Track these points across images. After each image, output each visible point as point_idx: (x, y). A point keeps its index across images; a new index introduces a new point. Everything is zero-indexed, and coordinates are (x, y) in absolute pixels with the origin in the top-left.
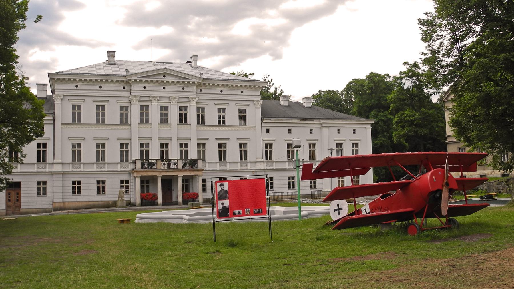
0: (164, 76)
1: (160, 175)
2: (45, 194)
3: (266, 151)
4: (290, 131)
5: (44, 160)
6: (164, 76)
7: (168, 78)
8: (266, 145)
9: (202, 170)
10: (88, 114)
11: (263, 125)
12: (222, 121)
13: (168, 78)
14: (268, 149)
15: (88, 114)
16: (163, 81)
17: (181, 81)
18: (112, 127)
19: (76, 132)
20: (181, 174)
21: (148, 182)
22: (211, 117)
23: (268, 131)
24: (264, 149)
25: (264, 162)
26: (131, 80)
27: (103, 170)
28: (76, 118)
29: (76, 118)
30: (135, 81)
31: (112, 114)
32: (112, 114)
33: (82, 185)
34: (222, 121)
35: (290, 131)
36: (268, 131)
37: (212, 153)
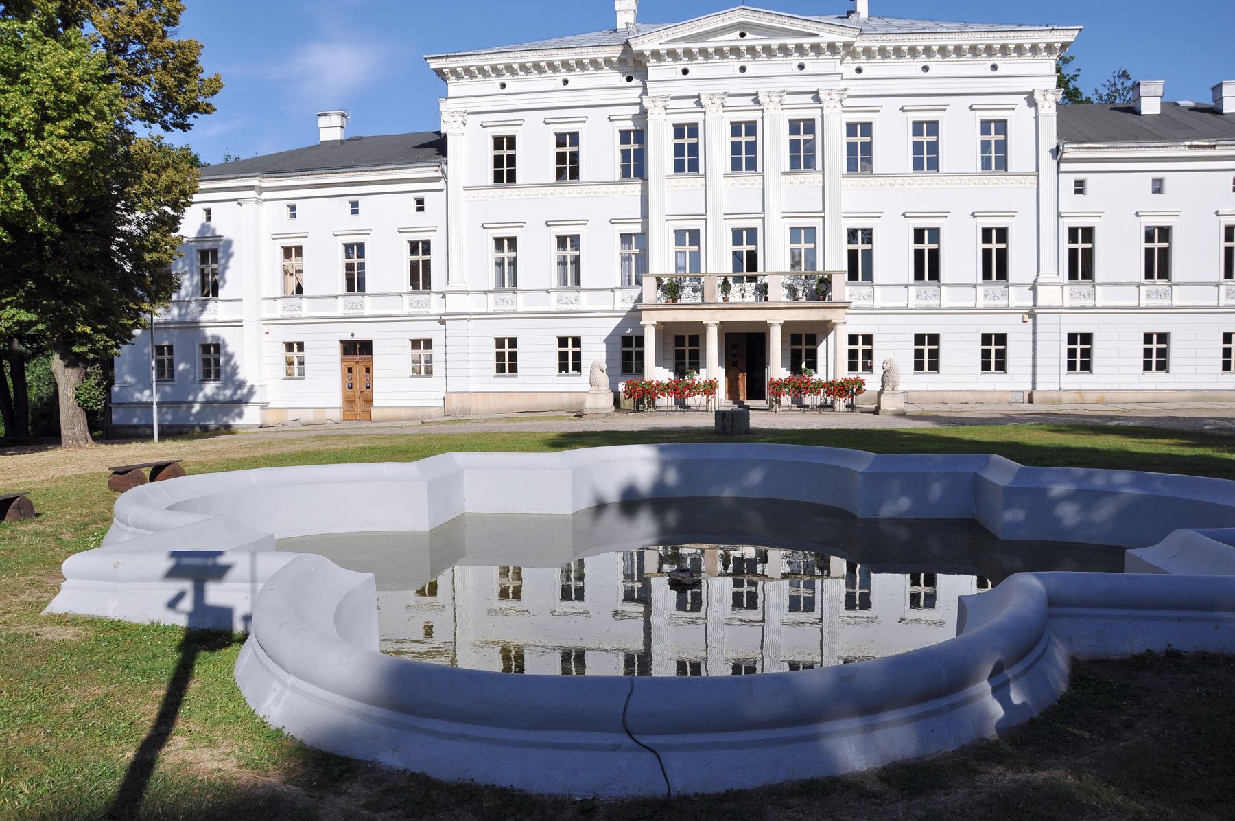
0: (742, 35)
1: (712, 320)
2: (429, 371)
3: (1073, 253)
4: (1158, 187)
5: (427, 284)
6: (742, 35)
7: (752, 39)
8: (1073, 233)
9: (844, 306)
10: (535, 158)
11: (1063, 167)
12: (926, 157)
13: (752, 39)
14: (1080, 246)
15: (535, 158)
16: (736, 51)
17: (791, 42)
18: (595, 188)
19: (506, 205)
20: (776, 319)
21: (813, 340)
22: (893, 145)
23: (1080, 188)
24: (1066, 246)
25: (1062, 286)
26: (641, 54)
27: (574, 307)
28: (505, 171)
29: (505, 171)
30: (656, 54)
31: (600, 154)
32: (600, 154)
33: (520, 350)
34: (926, 157)
35: (1158, 187)
36: (1080, 188)
37: (894, 256)
